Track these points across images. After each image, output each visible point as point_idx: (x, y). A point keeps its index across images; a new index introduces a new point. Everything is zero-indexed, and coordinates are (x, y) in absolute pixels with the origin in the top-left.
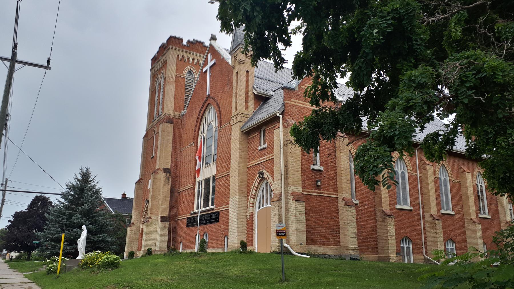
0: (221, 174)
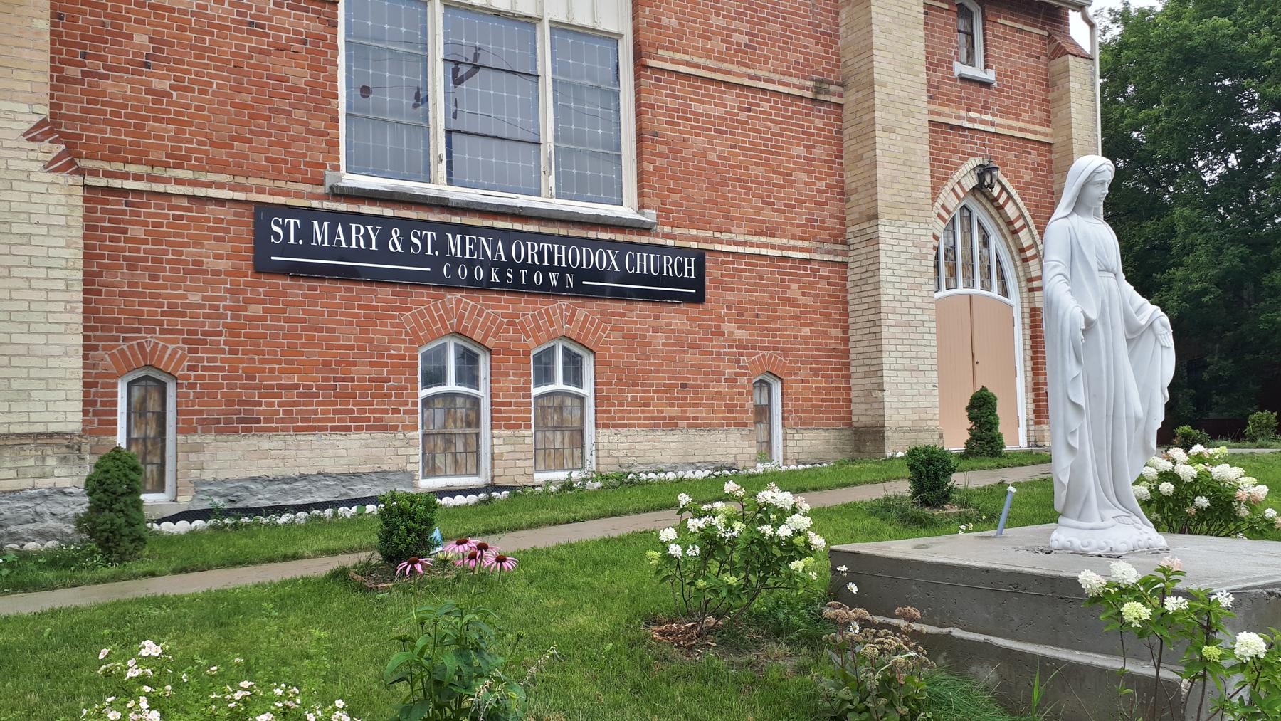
0: (696, 60)
